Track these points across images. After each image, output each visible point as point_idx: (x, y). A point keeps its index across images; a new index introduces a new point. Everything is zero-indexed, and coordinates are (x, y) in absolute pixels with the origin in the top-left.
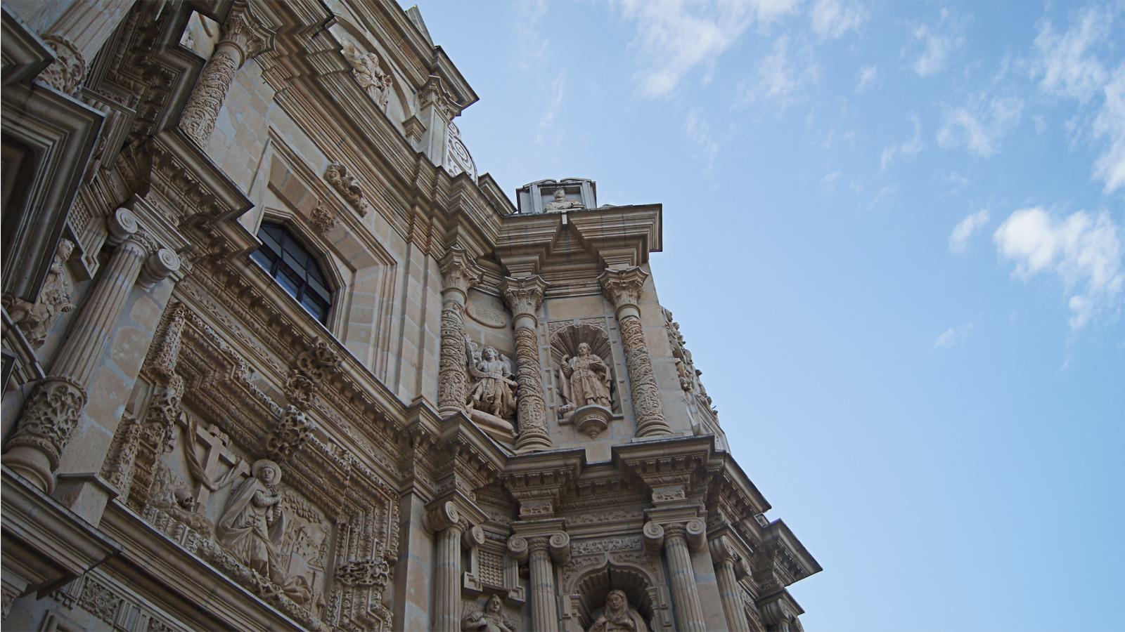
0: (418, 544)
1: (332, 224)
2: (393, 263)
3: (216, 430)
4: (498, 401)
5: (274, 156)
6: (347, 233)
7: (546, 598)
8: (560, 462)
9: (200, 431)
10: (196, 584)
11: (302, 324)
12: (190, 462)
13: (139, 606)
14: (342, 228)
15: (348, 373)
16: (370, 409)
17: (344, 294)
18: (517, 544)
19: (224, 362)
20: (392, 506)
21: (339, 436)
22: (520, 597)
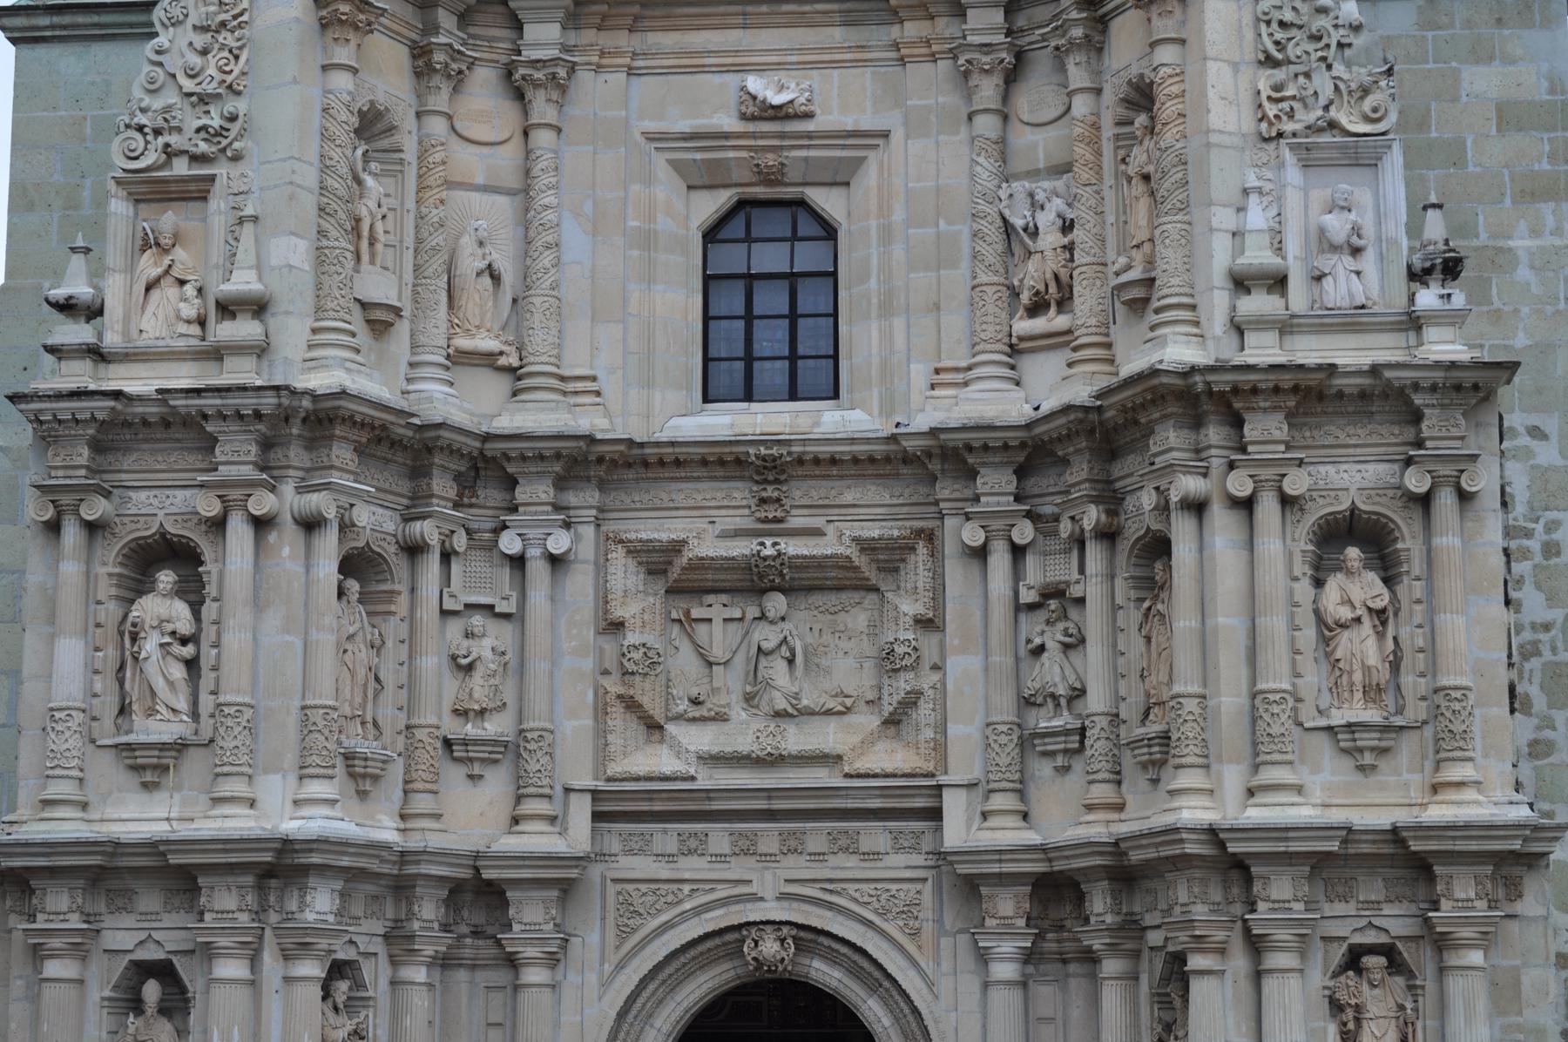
0: (956, 574)
1: (782, 164)
2: (885, 135)
3: (710, 599)
4: (1053, 289)
5: (669, 161)
6: (806, 159)
7: (1094, 590)
8: (1062, 421)
9: (695, 613)
10: (693, 799)
11: (727, 450)
12: (697, 647)
13: (665, 832)
14: (795, 158)
15: (804, 453)
16: (855, 460)
17: (841, 235)
18: (1065, 528)
19: (677, 547)
20: (922, 549)
21: (836, 511)
22: (1076, 591)
